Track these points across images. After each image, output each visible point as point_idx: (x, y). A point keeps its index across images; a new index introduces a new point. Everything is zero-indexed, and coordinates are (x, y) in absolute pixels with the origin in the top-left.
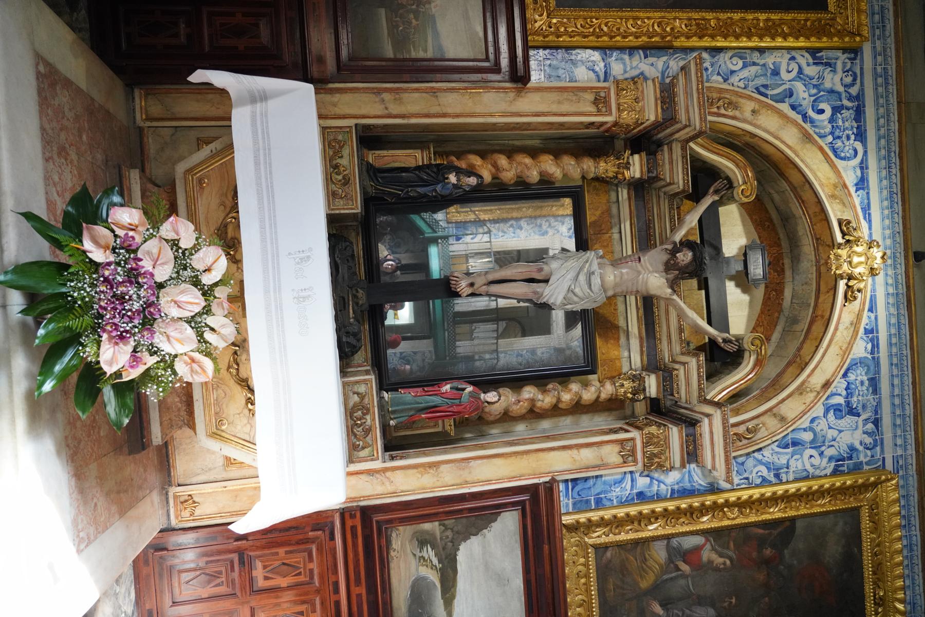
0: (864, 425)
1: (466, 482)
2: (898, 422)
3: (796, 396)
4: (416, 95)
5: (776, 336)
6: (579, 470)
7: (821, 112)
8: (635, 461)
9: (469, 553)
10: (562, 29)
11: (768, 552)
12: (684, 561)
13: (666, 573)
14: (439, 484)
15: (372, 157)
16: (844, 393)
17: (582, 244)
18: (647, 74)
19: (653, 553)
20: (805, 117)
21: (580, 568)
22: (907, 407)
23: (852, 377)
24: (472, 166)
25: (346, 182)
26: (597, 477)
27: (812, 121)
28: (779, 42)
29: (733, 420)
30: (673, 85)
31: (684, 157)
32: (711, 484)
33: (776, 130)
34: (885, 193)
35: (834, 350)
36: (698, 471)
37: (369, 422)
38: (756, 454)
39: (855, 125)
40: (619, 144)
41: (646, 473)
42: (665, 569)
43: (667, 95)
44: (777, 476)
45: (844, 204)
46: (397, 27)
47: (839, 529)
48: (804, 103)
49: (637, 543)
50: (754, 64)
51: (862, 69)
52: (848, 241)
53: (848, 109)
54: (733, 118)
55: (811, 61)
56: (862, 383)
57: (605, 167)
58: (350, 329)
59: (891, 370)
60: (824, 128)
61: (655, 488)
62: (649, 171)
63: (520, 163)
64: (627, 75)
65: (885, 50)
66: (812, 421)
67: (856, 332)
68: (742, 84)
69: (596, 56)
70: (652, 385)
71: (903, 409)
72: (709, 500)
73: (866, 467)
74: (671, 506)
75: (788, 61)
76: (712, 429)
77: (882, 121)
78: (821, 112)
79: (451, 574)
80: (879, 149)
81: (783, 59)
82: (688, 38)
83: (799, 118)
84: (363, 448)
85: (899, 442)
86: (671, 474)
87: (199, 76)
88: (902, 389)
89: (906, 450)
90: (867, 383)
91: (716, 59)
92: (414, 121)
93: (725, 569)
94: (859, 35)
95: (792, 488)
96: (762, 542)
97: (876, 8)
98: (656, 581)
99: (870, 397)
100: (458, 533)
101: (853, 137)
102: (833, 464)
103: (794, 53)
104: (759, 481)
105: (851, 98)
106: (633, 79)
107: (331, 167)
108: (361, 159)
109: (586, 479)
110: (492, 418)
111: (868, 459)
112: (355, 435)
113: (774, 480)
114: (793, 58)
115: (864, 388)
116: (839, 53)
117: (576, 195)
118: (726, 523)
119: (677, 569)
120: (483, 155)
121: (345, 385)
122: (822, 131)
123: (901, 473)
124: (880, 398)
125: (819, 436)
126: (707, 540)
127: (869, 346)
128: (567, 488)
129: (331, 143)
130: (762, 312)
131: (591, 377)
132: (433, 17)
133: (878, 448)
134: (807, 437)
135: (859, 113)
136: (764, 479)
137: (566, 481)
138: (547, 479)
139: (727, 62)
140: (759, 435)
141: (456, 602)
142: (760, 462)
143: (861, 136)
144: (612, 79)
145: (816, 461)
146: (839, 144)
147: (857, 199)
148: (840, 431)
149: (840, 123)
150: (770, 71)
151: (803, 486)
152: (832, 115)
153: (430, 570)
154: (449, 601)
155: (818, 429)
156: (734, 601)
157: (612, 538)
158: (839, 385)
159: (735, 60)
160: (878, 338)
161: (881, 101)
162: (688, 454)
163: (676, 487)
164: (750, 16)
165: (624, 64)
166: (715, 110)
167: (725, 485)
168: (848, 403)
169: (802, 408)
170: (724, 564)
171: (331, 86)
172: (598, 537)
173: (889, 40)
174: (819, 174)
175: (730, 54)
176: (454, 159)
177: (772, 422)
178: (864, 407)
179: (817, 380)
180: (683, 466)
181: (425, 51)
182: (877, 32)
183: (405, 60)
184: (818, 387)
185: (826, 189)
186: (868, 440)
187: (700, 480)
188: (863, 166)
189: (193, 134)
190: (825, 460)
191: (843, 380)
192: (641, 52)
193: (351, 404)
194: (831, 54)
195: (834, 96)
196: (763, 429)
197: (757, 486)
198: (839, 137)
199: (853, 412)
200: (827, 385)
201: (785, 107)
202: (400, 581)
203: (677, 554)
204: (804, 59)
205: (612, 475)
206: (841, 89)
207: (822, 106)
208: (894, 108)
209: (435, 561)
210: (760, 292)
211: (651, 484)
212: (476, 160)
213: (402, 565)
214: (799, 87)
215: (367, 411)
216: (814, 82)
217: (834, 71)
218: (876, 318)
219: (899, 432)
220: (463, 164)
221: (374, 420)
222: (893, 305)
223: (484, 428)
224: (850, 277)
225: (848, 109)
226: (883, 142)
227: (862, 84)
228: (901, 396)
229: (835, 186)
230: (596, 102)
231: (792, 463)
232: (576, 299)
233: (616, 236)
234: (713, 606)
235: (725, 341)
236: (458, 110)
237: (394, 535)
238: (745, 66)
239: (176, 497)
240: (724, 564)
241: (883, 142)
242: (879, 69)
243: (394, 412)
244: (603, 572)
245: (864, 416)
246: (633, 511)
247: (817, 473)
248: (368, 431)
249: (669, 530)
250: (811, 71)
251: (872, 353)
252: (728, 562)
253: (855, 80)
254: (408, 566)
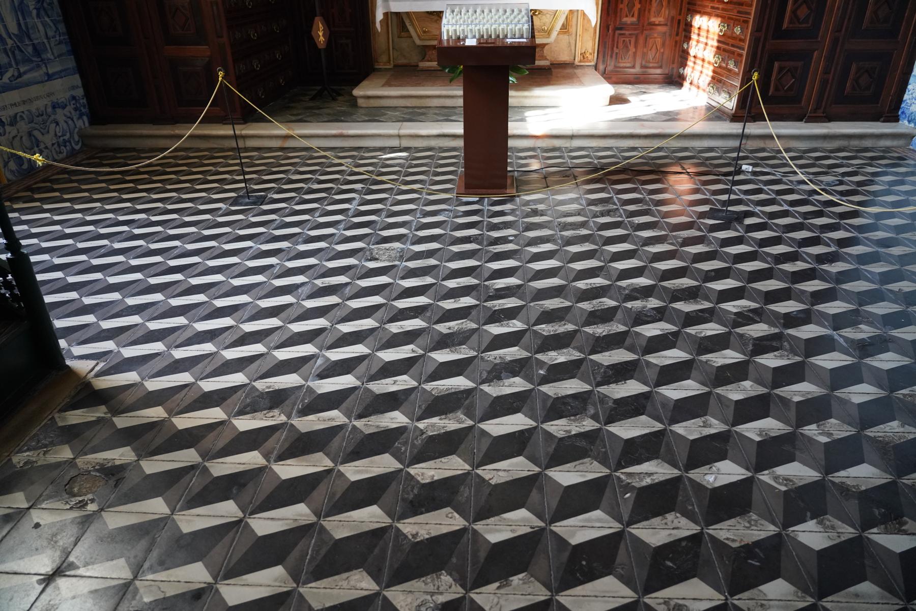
87: (378, 25)
239: (580, 61)
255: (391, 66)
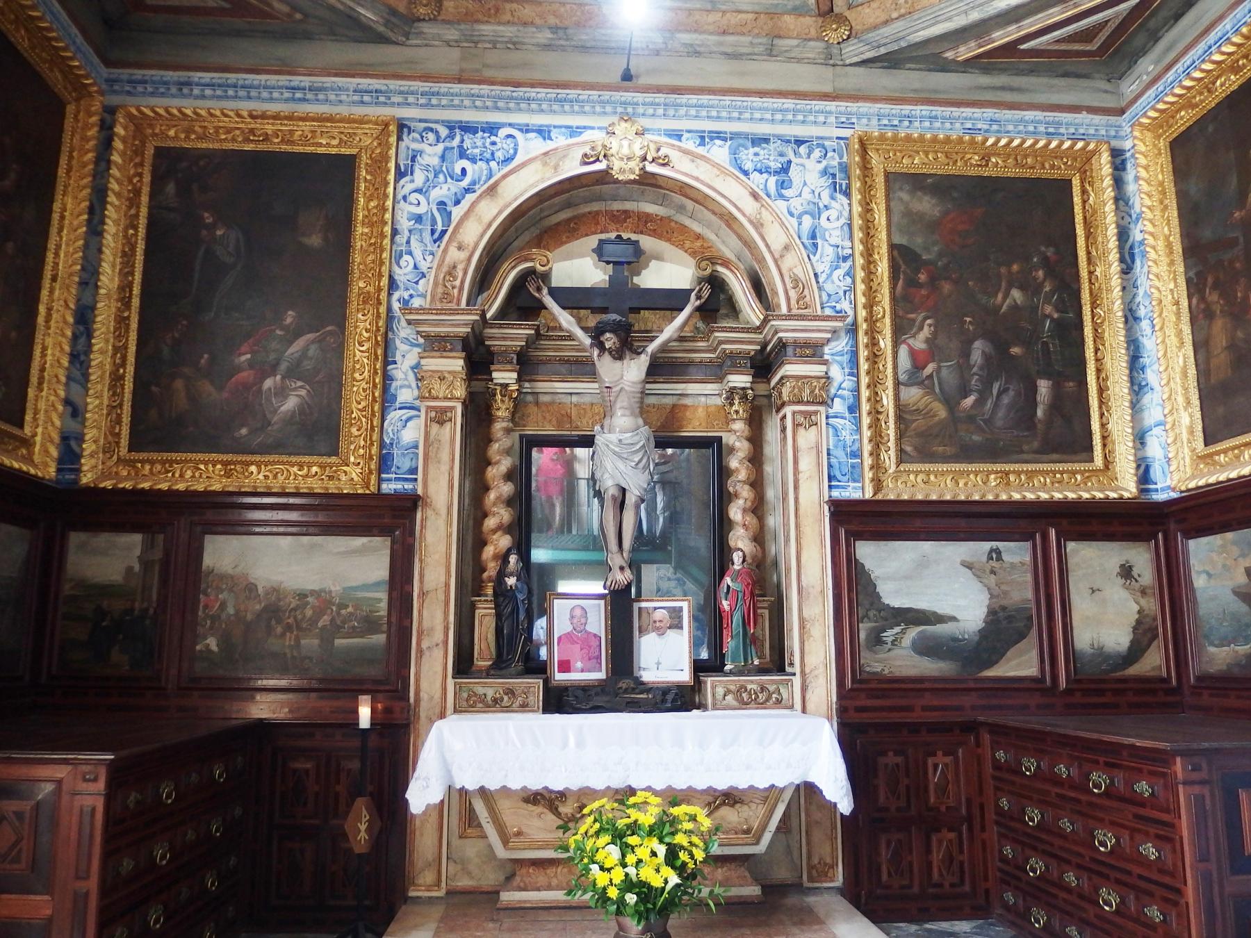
0: (801, 156)
1: (822, 592)
2: (800, 117)
3: (765, 231)
4: (425, 613)
5: (696, 227)
6: (820, 471)
7: (464, 171)
8: (816, 413)
9: (893, 595)
10: (361, 451)
11: (923, 277)
12: (923, 368)
13: (932, 388)
14: (821, 620)
15: (482, 663)
16: (765, 176)
17: (588, 441)
18: (414, 362)
19: (911, 401)
20: (467, 191)
21: (919, 479)
22: (786, 106)
23: (748, 166)
24: (495, 557)
25: (510, 692)
26: (829, 454)
27: (474, 183)
28: (388, 216)
29: (784, 310)
30: (427, 337)
31: (501, 326)
32: (848, 331)
33: (478, 225)
34: (555, 107)
35: (719, 184)
36: (833, 344)
37: (754, 687)
38: (821, 280)
39: (480, 134)
40: (478, 386)
41: (829, 402)
42: (930, 390)
43: (436, 344)
44: (845, 259)
45: (565, 156)
46: (354, 627)
47: (905, 196)
48: (454, 190)
49: (899, 418)
50: (408, 242)
51: (421, 121)
52: (605, 156)
53: (462, 141)
54: (465, 273)
55: (408, 178)
56: (756, 154)
57: (502, 410)
58: (659, 698)
59: (746, 120)
60: (482, 171)
61: (845, 393)
62: (511, 362)
63: (494, 504)
64: (414, 385)
65: (401, 93)
66: (792, 215)
67: (702, 158)
68: (429, 258)
69: (394, 416)
70: (741, 380)
71: (787, 110)
72: (863, 339)
73: (845, 159)
74: (865, 380)
75: (411, 202)
76: (789, 330)
77: (478, 103)
78: (464, 171)
79: (909, 615)
80: (509, 109)
81: (405, 210)
82: (379, 316)
83: (470, 198)
84: (779, 693)
85: (821, 119)
86: (831, 374)
88: (766, 109)
89: (830, 112)
90: (757, 149)
91: (401, 285)
92: (452, 618)
93: (936, 327)
94: (387, 125)
95: (859, 247)
96: (912, 283)
97: (356, 98)
98: (940, 401)
99: (772, 146)
100: (872, 604)
101: (493, 138)
102: (839, 196)
103: (400, 197)
104: (849, 280)
105: (451, 137)
106: (417, 379)
107: (495, 705)
108: (488, 673)
109: (830, 466)
110: (760, 555)
111: (836, 156)
112: (767, 700)
113: (849, 263)
114: (405, 198)
115: (762, 152)
116: (403, 145)
117: (531, 443)
118: (888, 320)
119: (930, 377)
120: (481, 543)
121: (715, 708)
122: (485, 172)
123: (854, 120)
124: (774, 136)
125: (808, 208)
126: (904, 342)
127: (718, 142)
128: (837, 487)
129: (470, 705)
130: (669, 240)
131: (724, 441)
132: (344, 589)
133: (827, 143)
134: (807, 221)
135: (469, 129)
136: (847, 274)
137: (830, 487)
138: (826, 508)
139: (403, 273)
140: (801, 275)
141: (940, 611)
142: (829, 276)
143: (492, 129)
144: (417, 403)
145: (833, 214)
146: (499, 155)
147: (559, 140)
148: (805, 184)
149: (477, 151)
150: (417, 226)
151: (858, 235)
152: (468, 159)
153: (906, 636)
154: (940, 619)
155: (801, 209)
156: (968, 319)
157: (892, 444)
158: (757, 179)
159: (402, 263)
160: (710, 132)
161: (456, 102)
162: (813, 355)
163: (847, 371)
164: (359, 244)
165: (401, 387)
166: (456, 291)
167: (850, 320)
168: (776, 173)
169: (776, 225)
170: (930, 326)
171: (412, 700)
172: (889, 458)
173: (392, 87)
174: (531, 182)
175: (396, 268)
176: (485, 575)
177: (789, 262)
178: (781, 155)
179: (749, 206)
180: (825, 363)
181: (380, 600)
182: (382, 99)
183: (389, 623)
184: (757, 205)
185: (548, 175)
186: (817, 153)
187: (842, 344)
188: (526, 129)
189: (456, 842)
190: (833, 204)
191: (751, 176)
192: (390, 367)
193: (735, 703)
194: (402, 155)
195: (448, 155)
196: (795, 271)
197: (854, 282)
198: (493, 154)
199: (785, 169)
200: (755, 196)
201: (457, 212)
202: (914, 667)
203: (915, 376)
204: (407, 186)
205: (828, 438)
206: (441, 147)
207: (458, 171)
208: (465, 88)
209: (897, 629)
210: (647, 242)
211: (842, 397)
212: (489, 551)
213: (898, 663)
214: (437, 194)
215: (742, 688)
216: (431, 176)
217: (421, 152)
218: (689, 131)
219: (811, 118)
220: (492, 569)
221: (752, 682)
222: (676, 111)
223: (769, 561)
224: (644, 159)
225: (462, 141)
226: (501, 104)
227: (437, 122)
228: (775, 111)
229: (545, 164)
230: (441, 423)
231: (833, 241)
232: (644, 461)
233: (575, 399)
234: (971, 342)
235: (699, 297)
236: (443, 571)
237: (868, 669)
238: (410, 253)
240: (930, 326)
241: (501, 104)
242: (422, 101)
243: (746, 660)
244: (926, 455)
245: (791, 156)
246: (866, 421)
247: (846, 214)
248: (763, 689)
249: (890, 383)
250: (419, 178)
251: (725, 140)
252: (929, 321)
253: (431, 130)
254: (901, 658)
255: (441, 893)
